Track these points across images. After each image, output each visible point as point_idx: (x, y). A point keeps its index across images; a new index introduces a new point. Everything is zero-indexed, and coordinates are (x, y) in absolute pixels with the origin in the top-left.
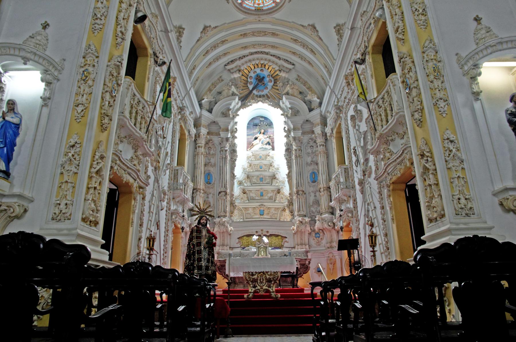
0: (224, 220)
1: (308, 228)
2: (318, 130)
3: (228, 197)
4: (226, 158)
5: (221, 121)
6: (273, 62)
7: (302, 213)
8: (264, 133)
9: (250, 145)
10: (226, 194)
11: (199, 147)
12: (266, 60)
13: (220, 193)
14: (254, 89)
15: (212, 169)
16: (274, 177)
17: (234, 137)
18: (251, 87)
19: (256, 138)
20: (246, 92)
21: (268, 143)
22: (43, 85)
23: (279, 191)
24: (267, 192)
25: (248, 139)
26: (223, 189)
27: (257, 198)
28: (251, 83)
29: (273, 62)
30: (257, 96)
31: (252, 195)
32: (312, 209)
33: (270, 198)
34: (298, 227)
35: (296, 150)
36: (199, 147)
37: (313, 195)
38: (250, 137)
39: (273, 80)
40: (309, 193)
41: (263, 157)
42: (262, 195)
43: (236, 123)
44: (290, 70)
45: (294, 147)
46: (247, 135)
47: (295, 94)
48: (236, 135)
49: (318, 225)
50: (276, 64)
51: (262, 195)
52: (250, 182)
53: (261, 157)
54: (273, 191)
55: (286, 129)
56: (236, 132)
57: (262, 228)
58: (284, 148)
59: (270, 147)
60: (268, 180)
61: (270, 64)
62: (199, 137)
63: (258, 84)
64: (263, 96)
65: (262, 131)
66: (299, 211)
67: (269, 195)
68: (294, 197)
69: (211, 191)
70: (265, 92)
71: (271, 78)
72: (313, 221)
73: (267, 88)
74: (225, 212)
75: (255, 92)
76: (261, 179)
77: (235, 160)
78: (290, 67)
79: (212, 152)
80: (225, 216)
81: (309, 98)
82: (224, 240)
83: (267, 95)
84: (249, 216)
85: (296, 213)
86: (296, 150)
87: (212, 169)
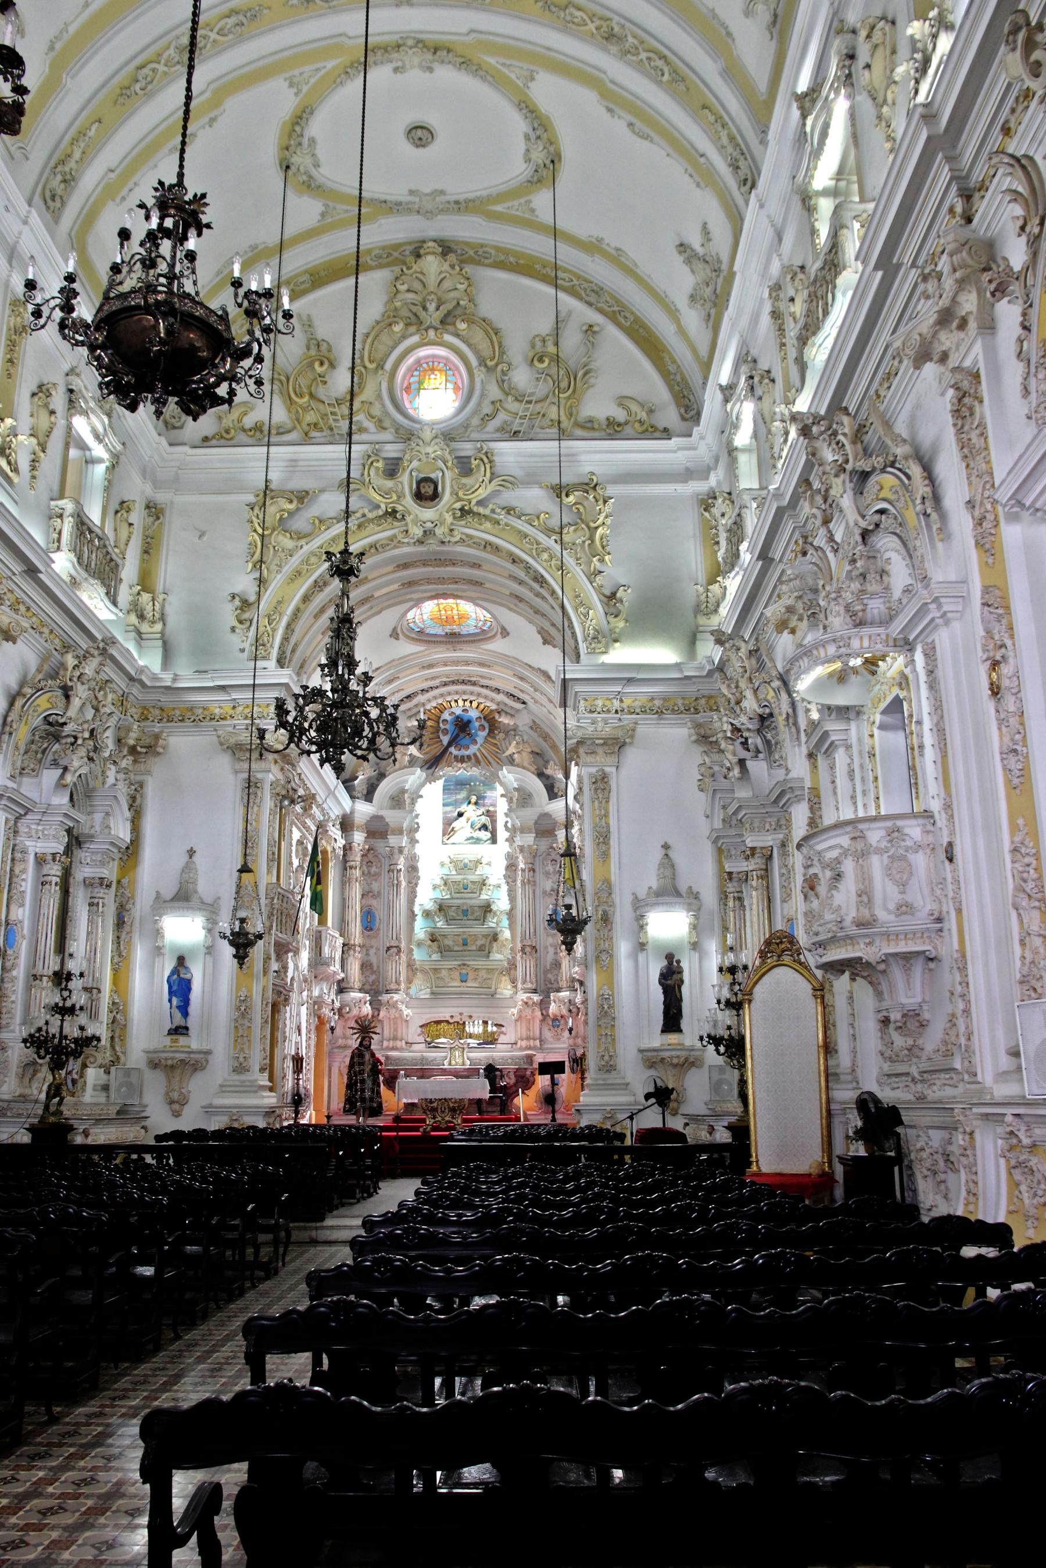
0: (396, 997)
1: (538, 1014)
2: (561, 835)
3: (403, 956)
4: (398, 885)
5: (391, 816)
6: (486, 697)
7: (529, 986)
8: (476, 803)
9: (448, 829)
10: (399, 951)
11: (351, 867)
12: (472, 693)
13: (388, 949)
14: (450, 744)
15: (374, 902)
16: (487, 909)
17: (413, 841)
18: (445, 739)
19: (460, 815)
20: (436, 750)
21: (484, 827)
22: (203, 933)
23: (495, 937)
24: (475, 937)
25: (445, 813)
26: (393, 944)
27: (456, 948)
28: (445, 732)
29: (486, 697)
30: (456, 757)
31: (449, 942)
32: (550, 976)
33: (481, 949)
34: (520, 1011)
35: (523, 870)
36: (351, 867)
37: (551, 950)
38: (448, 809)
39: (486, 725)
40: (546, 948)
41: (471, 865)
42: (465, 944)
43: (417, 816)
44: (518, 711)
45: (522, 865)
46: (444, 805)
47: (526, 764)
48: (418, 836)
49: (553, 1008)
50: (492, 700)
51: (465, 944)
52: (445, 916)
53: (466, 866)
54: (485, 936)
55: (509, 825)
56: (417, 830)
57: (461, 1010)
58: (504, 863)
59: (488, 835)
60: (478, 913)
61: (481, 700)
62: (351, 848)
63: (457, 736)
64: (469, 757)
65: (474, 799)
66: (524, 982)
67: (479, 943)
68: (518, 957)
69: (373, 942)
70: (473, 749)
71: (483, 722)
72: (544, 1004)
73: (475, 742)
74: (398, 983)
75: (452, 749)
76: (465, 913)
77: (416, 885)
78: (519, 706)
79: (374, 870)
80: (397, 991)
81: (549, 772)
82: (396, 1030)
83: (475, 755)
84: (441, 984)
85: (520, 986)
86: (523, 870)
87: (374, 902)
